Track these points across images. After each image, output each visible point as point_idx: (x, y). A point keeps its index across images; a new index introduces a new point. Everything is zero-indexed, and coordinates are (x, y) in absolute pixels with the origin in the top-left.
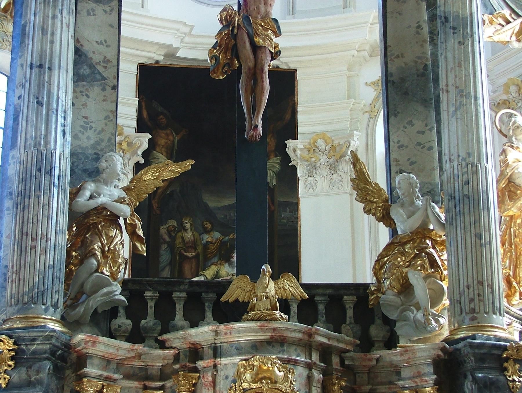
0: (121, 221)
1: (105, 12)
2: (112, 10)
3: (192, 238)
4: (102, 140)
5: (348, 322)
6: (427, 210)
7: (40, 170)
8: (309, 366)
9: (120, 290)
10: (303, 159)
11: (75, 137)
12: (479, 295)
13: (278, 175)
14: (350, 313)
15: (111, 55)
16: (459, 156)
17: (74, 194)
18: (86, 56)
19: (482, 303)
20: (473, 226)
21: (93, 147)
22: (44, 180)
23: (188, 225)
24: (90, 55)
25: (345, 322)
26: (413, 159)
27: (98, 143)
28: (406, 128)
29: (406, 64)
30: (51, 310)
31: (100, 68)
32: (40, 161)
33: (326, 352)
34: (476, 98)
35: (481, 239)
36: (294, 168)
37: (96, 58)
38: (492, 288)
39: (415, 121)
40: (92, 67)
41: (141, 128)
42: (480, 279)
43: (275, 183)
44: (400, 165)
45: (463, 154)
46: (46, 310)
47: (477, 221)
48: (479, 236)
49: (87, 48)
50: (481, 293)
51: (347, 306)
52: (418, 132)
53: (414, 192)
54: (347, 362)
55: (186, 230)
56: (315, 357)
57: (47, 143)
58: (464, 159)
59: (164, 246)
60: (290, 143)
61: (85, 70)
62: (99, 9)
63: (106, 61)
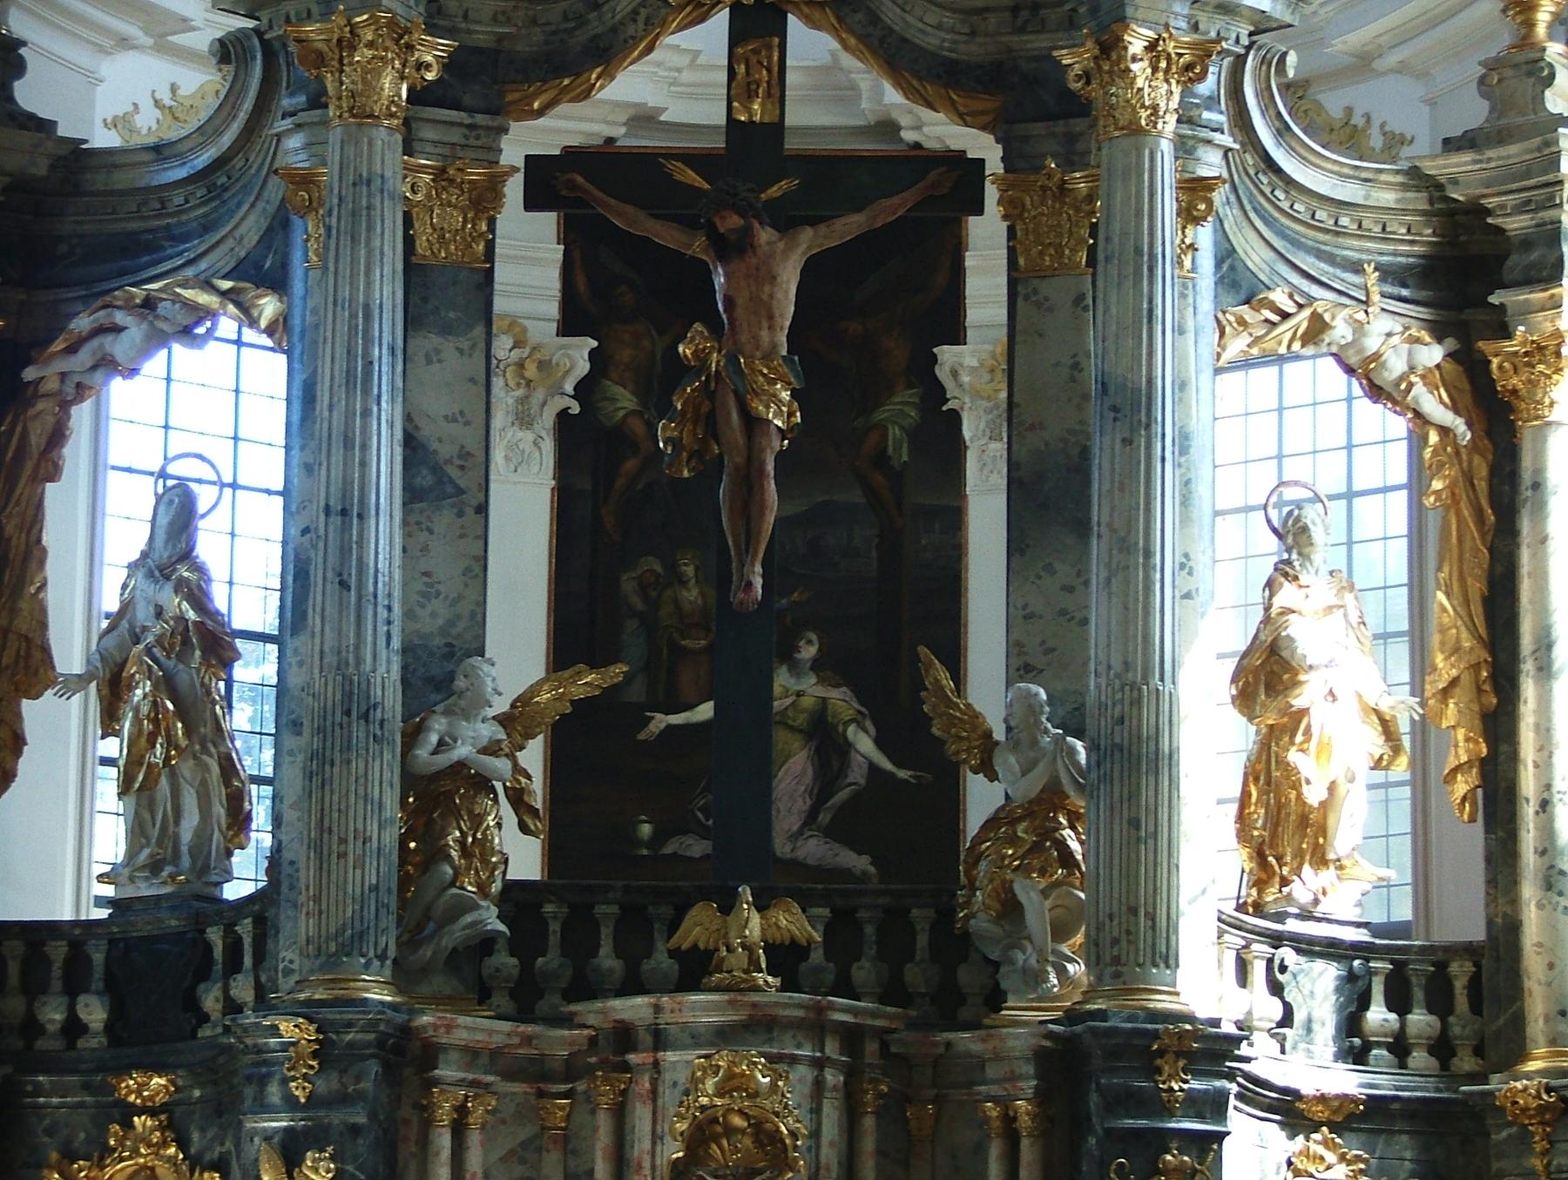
0: (498, 786)
1: (461, 351)
2: (473, 347)
3: (700, 602)
4: (459, 617)
5: (918, 958)
6: (1055, 759)
7: (348, 713)
8: (819, 1064)
9: (494, 911)
10: (977, 395)
11: (409, 615)
12: (1128, 932)
13: (915, 436)
14: (922, 940)
15: (473, 443)
16: (1109, 667)
17: (412, 736)
18: (424, 447)
19: (1132, 948)
20: (1125, 805)
21: (443, 631)
22: (358, 731)
23: (690, 571)
24: (435, 445)
25: (912, 959)
26: (1050, 644)
27: (451, 623)
28: (1040, 578)
29: (1047, 444)
30: (377, 963)
31: (452, 471)
32: (348, 696)
33: (852, 1037)
34: (1148, 554)
35: (1138, 828)
36: (955, 418)
37: (445, 451)
38: (1153, 920)
39: (1058, 566)
40: (436, 469)
41: (570, 325)
42: (1132, 904)
43: (905, 458)
44: (1025, 654)
45: (1117, 665)
46: (367, 966)
47: (1133, 796)
48: (1135, 823)
49: (427, 431)
50: (1132, 929)
51: (918, 927)
52: (1064, 588)
53: (1038, 723)
54: (893, 1049)
55: (683, 583)
56: (832, 1049)
57: (359, 661)
58: (1118, 676)
59: (631, 625)
60: (946, 353)
61: (425, 479)
62: (448, 346)
63: (465, 455)
